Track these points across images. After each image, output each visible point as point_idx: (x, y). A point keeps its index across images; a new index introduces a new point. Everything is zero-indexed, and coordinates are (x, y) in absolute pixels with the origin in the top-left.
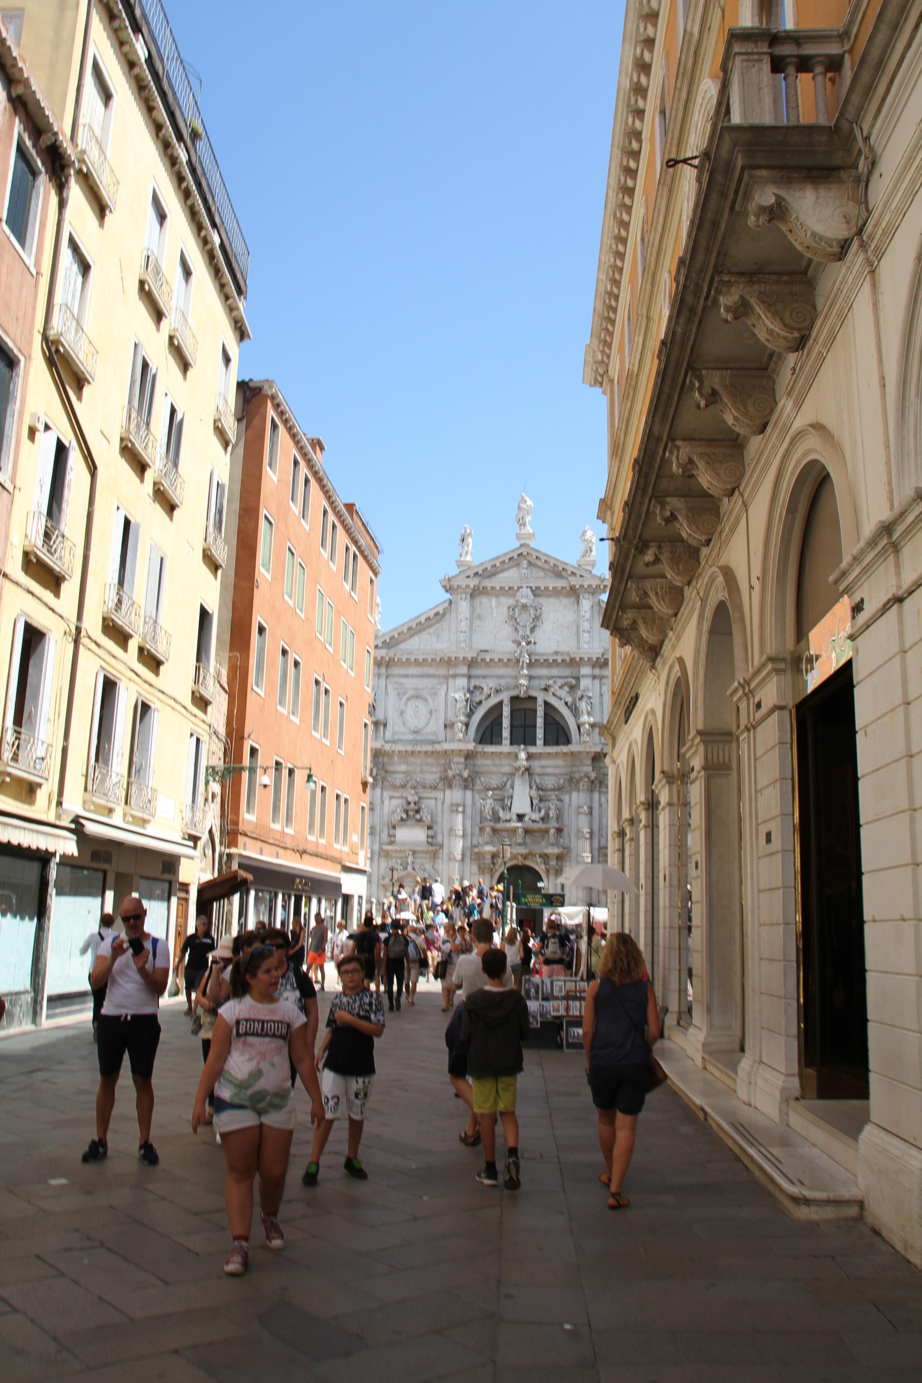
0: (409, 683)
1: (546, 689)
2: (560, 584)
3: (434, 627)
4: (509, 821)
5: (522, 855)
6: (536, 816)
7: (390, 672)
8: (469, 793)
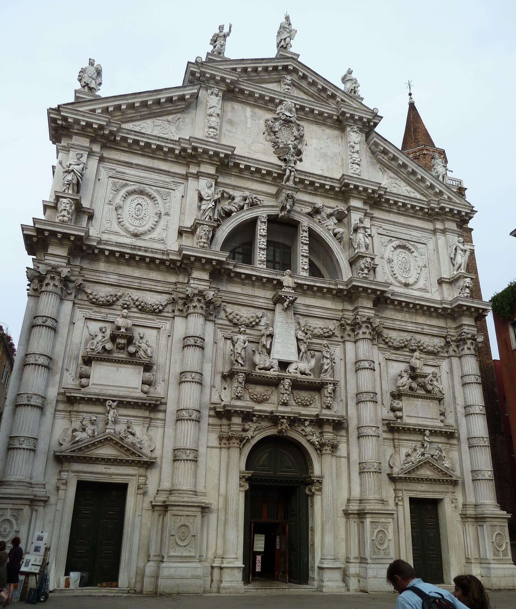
2: (327, 110)
3: (175, 116)
5: (289, 417)
6: (304, 366)
8: (210, 326)
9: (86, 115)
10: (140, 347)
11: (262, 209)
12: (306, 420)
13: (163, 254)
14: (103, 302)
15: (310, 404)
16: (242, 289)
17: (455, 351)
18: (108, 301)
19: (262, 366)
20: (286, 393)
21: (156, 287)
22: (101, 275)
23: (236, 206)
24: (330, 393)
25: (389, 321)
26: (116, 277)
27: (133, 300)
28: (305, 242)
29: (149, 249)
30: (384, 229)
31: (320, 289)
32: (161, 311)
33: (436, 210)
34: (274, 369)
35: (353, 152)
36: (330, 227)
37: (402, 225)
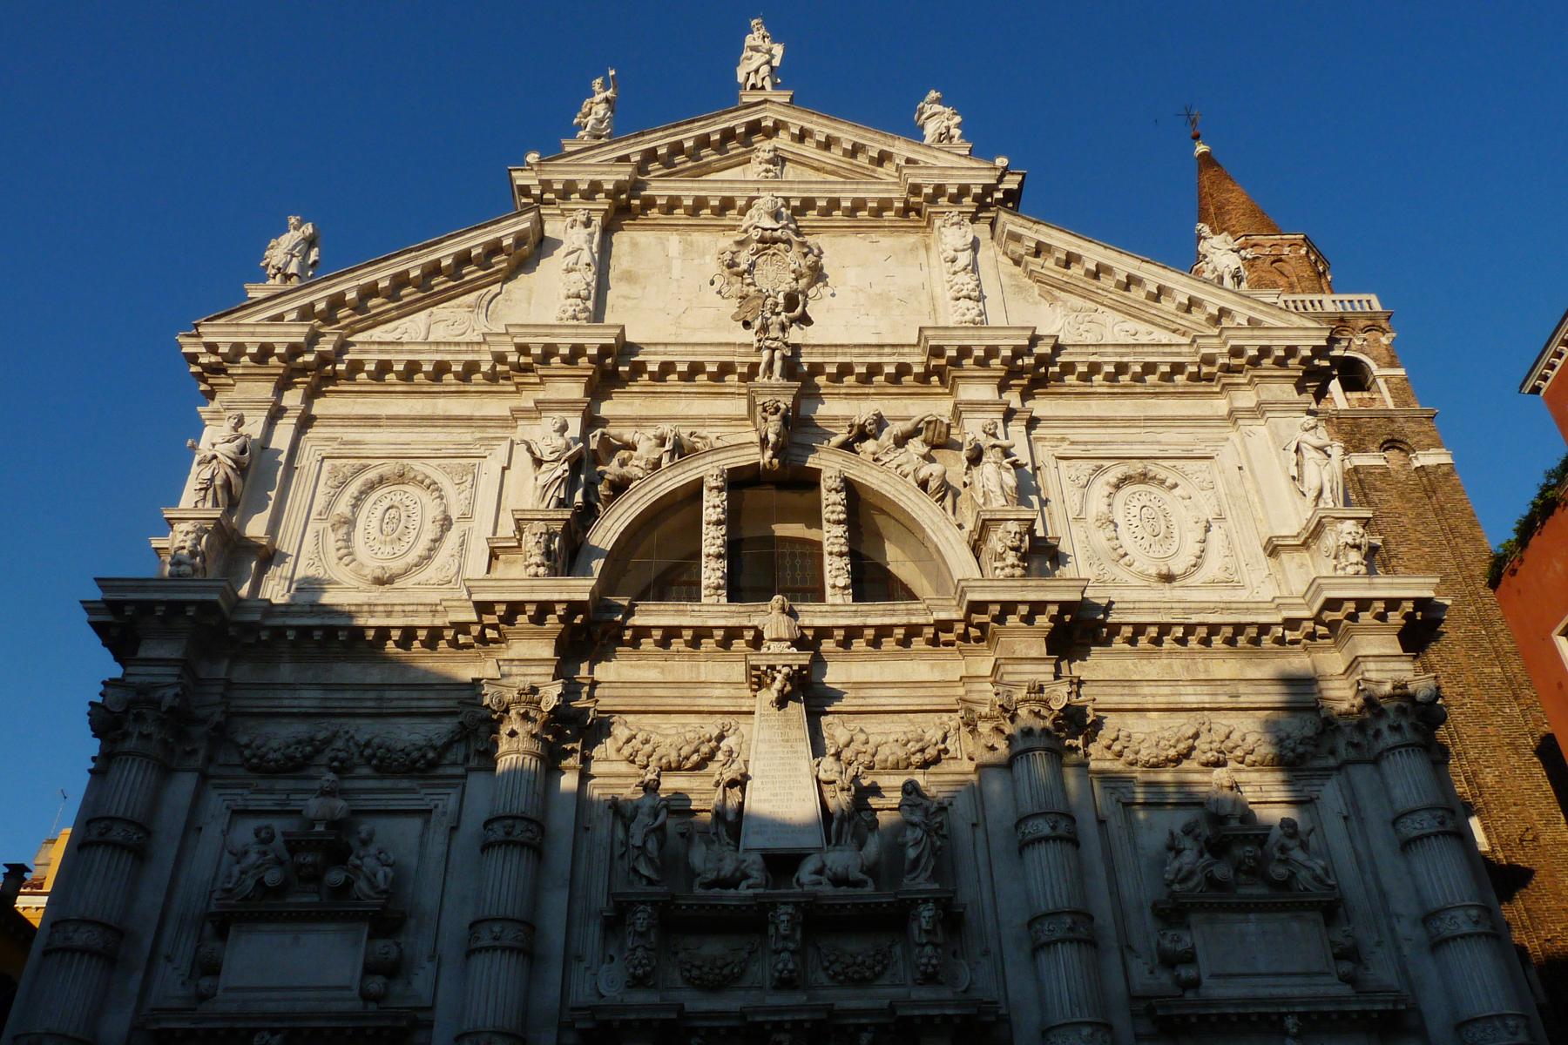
0: (377, 440)
1: (847, 446)
2: (872, 193)
4: (731, 883)
5: (797, 1024)
7: (319, 407)
9: (258, 329)
10: (357, 867)
11: (709, 459)
12: (864, 1028)
13: (434, 613)
14: (276, 761)
15: (878, 976)
16: (663, 672)
17: (1356, 746)
18: (291, 758)
19: (711, 876)
20: (785, 949)
21: (422, 703)
22: (279, 693)
23: (642, 464)
24: (927, 932)
25: (1119, 690)
26: (318, 694)
27: (357, 744)
28: (834, 517)
29: (397, 608)
30: (1072, 443)
31: (883, 631)
32: (433, 764)
33: (1220, 361)
34: (751, 881)
35: (955, 273)
36: (908, 468)
37: (1129, 421)
